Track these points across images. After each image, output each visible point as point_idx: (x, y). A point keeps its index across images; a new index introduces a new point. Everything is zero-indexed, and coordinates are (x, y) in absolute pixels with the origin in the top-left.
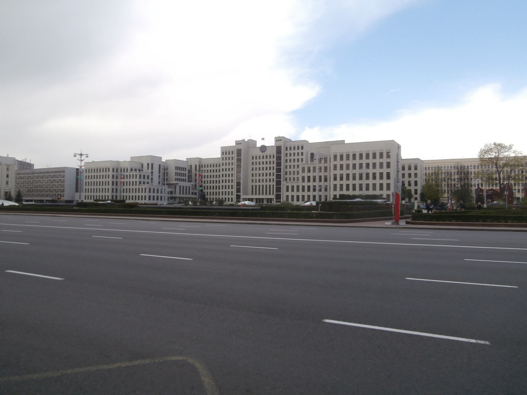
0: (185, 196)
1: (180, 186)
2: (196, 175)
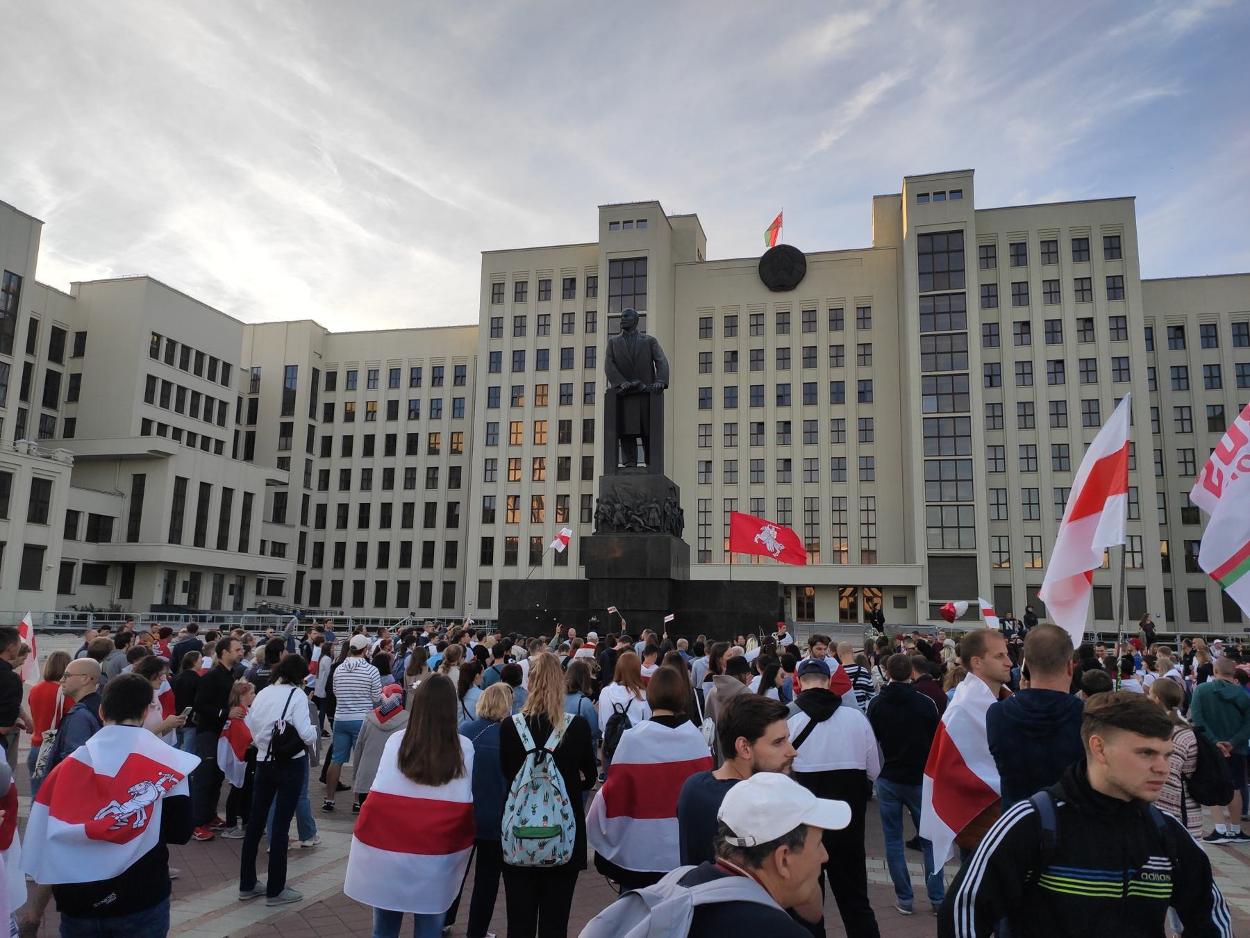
0: (209, 557)
1: (181, 483)
2: (287, 430)
